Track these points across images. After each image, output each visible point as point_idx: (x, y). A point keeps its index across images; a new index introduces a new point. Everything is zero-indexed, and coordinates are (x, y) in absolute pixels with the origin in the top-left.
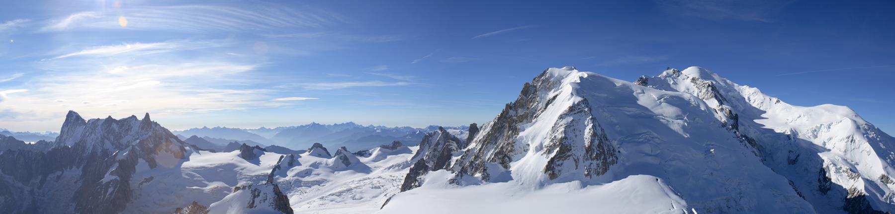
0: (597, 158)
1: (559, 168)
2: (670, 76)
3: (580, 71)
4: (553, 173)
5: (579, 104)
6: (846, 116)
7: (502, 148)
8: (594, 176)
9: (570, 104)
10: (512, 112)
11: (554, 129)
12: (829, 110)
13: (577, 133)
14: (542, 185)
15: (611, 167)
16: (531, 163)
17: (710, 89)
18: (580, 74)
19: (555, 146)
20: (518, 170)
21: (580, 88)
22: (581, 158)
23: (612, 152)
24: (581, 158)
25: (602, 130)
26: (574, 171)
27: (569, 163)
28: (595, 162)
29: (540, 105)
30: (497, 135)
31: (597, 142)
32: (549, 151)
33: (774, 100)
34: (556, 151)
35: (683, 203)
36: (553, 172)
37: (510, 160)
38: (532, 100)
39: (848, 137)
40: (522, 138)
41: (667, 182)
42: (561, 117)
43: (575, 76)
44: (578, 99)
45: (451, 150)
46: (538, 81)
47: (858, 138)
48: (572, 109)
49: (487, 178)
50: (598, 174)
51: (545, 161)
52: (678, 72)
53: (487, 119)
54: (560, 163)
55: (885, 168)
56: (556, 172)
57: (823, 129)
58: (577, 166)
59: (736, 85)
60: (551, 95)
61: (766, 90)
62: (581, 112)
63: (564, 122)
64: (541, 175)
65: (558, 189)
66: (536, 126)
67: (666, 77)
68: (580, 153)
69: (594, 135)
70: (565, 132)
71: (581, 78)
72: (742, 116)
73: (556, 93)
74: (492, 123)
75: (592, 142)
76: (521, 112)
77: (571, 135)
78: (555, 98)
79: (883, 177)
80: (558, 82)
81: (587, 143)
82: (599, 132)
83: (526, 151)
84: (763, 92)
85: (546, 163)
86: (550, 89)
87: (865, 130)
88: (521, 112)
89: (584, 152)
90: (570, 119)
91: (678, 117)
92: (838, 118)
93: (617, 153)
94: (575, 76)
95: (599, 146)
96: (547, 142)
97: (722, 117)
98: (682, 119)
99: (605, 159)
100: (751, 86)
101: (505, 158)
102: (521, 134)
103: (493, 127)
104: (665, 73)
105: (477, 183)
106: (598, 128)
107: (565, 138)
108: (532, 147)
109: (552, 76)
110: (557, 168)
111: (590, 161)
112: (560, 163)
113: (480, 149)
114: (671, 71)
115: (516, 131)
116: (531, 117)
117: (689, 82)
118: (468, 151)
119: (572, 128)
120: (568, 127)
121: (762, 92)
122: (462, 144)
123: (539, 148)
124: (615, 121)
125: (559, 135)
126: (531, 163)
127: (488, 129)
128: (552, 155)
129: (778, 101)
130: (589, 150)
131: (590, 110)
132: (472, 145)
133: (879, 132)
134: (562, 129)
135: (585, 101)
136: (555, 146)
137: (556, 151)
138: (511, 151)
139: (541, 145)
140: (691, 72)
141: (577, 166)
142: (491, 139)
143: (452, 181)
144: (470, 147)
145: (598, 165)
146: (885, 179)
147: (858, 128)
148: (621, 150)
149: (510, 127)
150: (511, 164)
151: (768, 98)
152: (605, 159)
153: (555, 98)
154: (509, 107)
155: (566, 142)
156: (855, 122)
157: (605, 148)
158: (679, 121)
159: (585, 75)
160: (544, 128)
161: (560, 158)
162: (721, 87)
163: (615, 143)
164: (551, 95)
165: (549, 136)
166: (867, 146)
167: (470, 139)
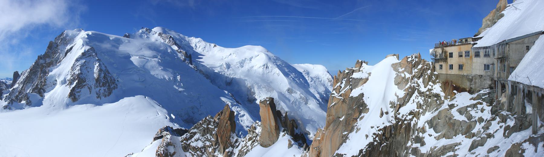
0: (104, 85)
1: (79, 94)
2: (144, 33)
3: (86, 31)
4: (75, 97)
5: (88, 51)
6: (261, 52)
7: (37, 85)
8: (103, 98)
9: (82, 51)
10: (41, 61)
11: (73, 68)
12: (249, 49)
13: (89, 70)
14: (68, 106)
15: (114, 91)
16: (60, 92)
17: (171, 39)
18: (87, 32)
19: (74, 80)
20: (50, 97)
21: (90, 40)
22: (93, 87)
23: (113, 81)
24: (93, 87)
25: (105, 67)
26: (89, 95)
27: (84, 91)
28: (102, 88)
29: (61, 55)
30: (33, 77)
31: (103, 75)
32: (71, 83)
33: (213, 45)
34: (75, 83)
35: (165, 111)
36: (74, 98)
37: (45, 92)
38: (55, 53)
39: (264, 65)
40: (52, 77)
41: (152, 97)
42: (77, 60)
43: (83, 34)
44: (87, 48)
45: (2, 90)
46: (58, 39)
47: (270, 65)
48: (84, 54)
49: (29, 104)
50: (105, 96)
51: (68, 90)
52: (149, 30)
53: (25, 69)
54: (78, 90)
55: (290, 83)
56: (77, 97)
57: (247, 62)
58: (90, 92)
59: (186, 37)
60: (68, 47)
61: (207, 39)
62: (90, 56)
63: (79, 63)
64: (66, 100)
65: (78, 109)
66: (60, 67)
67: (141, 33)
68: (92, 83)
69: (100, 70)
70: (81, 70)
71: (88, 35)
72: (192, 56)
73: (72, 45)
74: (29, 70)
75: (99, 75)
76: (48, 60)
77: (85, 71)
78: (71, 48)
79: (288, 90)
80: (72, 39)
81: (96, 76)
82: (104, 68)
83: (55, 84)
84: (205, 40)
85: (70, 91)
86: (67, 44)
87: (275, 60)
88: (48, 60)
89: (95, 82)
90: (83, 61)
91: (155, 57)
92: (256, 54)
93: (116, 82)
94: (83, 34)
95: (104, 77)
96: (69, 77)
97: (181, 56)
98: (157, 58)
99: (109, 86)
100: (197, 37)
101: (41, 91)
102: (50, 74)
103: (30, 72)
104: (140, 31)
105: (21, 108)
106: (102, 66)
107: (81, 73)
108: (59, 81)
109: (67, 35)
110: (77, 94)
111: (99, 88)
112: (78, 90)
113: (22, 87)
114: (144, 30)
115: (45, 73)
116: (56, 62)
117: (156, 36)
118: (14, 89)
119: (85, 67)
120: (82, 66)
121: (204, 40)
122: (8, 87)
123: (64, 82)
124: (112, 61)
125: (77, 72)
126: (60, 92)
127: (26, 74)
128: (73, 86)
129: (215, 46)
130: (98, 80)
131: (96, 54)
132: (16, 86)
133: (283, 62)
134: (78, 68)
135: (92, 49)
136: (74, 80)
137: (75, 83)
138: (45, 85)
139: (65, 79)
140: (157, 30)
141: (90, 92)
142: (28, 80)
143: (6, 107)
144: (15, 87)
145: (105, 90)
146: (290, 91)
147: (270, 59)
148: (119, 80)
149: (41, 71)
150: (45, 94)
151: (208, 44)
152: (109, 86)
153: (71, 48)
154: (40, 58)
155: (82, 76)
156: (267, 55)
157: (109, 79)
158: (155, 59)
159: (90, 33)
160: (65, 68)
161: (79, 87)
162: (177, 39)
163: (115, 75)
164: (68, 47)
165: (70, 73)
166: (277, 71)
167: (15, 81)
